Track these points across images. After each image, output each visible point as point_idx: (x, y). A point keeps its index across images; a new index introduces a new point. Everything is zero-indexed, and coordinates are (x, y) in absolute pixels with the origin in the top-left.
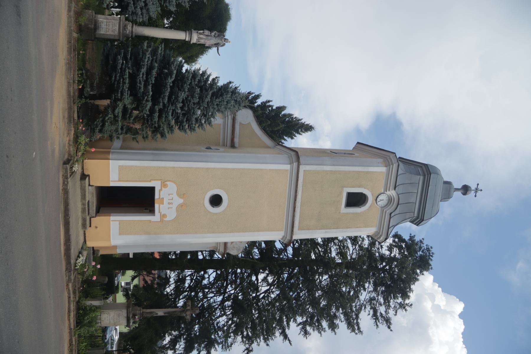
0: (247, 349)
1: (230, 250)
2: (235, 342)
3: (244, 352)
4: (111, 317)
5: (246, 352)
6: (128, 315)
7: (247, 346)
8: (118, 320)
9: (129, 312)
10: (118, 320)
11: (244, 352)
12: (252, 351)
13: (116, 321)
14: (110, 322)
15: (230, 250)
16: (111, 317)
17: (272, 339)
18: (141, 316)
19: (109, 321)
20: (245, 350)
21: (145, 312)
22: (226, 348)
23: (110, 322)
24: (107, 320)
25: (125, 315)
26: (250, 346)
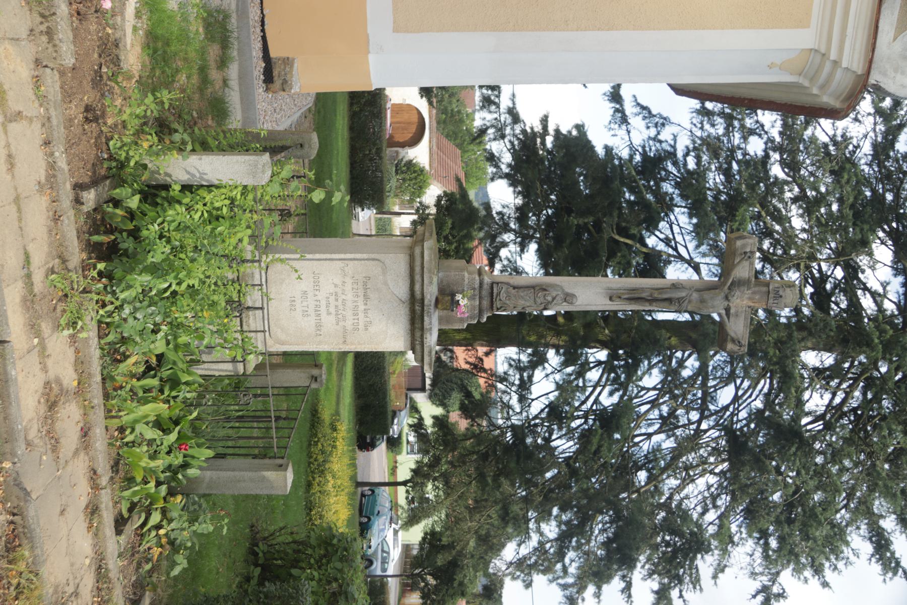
0: (765, 589)
1: (885, 74)
2: (725, 566)
3: (754, 597)
4: (321, 296)
5: (760, 598)
6: (417, 287)
7: (765, 579)
8: (361, 315)
9: (418, 269)
10: (361, 315)
11: (754, 597)
12: (781, 596)
13: (349, 324)
14: (319, 326)
15: (885, 74)
16: (321, 296)
17: (836, 568)
18: (486, 303)
19: (312, 320)
20: (758, 592)
21: (508, 284)
22: (692, 583)
23: (319, 326)
24: (305, 314)
25: (401, 289)
26: (774, 582)
